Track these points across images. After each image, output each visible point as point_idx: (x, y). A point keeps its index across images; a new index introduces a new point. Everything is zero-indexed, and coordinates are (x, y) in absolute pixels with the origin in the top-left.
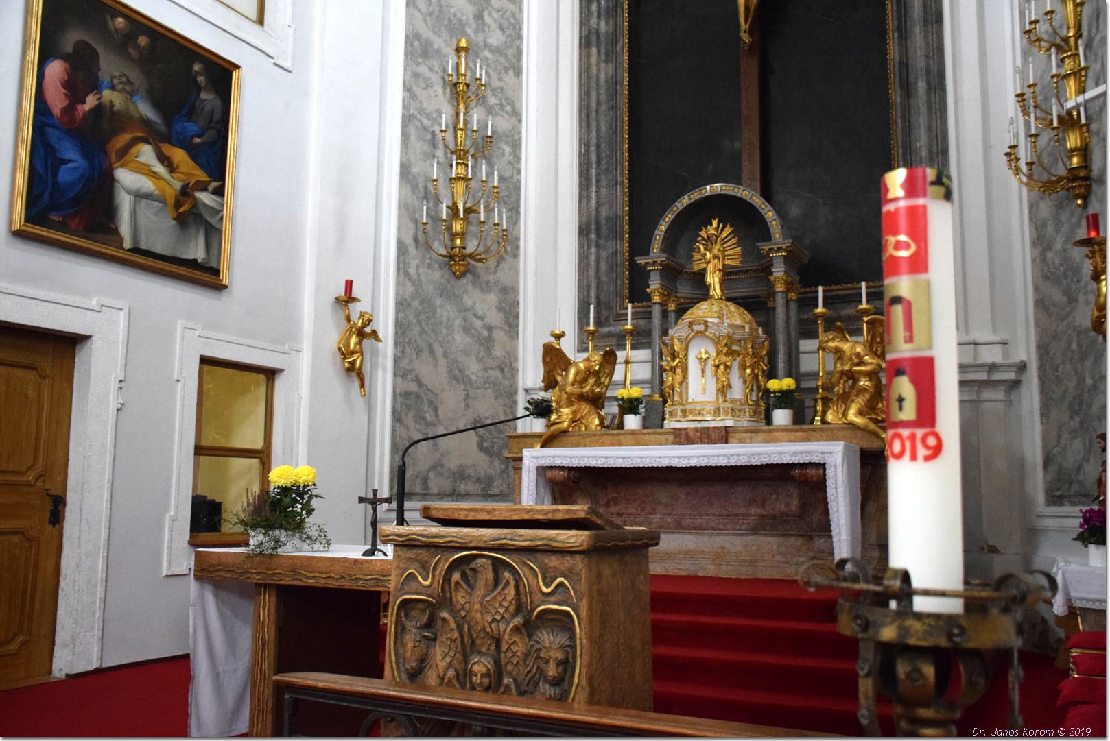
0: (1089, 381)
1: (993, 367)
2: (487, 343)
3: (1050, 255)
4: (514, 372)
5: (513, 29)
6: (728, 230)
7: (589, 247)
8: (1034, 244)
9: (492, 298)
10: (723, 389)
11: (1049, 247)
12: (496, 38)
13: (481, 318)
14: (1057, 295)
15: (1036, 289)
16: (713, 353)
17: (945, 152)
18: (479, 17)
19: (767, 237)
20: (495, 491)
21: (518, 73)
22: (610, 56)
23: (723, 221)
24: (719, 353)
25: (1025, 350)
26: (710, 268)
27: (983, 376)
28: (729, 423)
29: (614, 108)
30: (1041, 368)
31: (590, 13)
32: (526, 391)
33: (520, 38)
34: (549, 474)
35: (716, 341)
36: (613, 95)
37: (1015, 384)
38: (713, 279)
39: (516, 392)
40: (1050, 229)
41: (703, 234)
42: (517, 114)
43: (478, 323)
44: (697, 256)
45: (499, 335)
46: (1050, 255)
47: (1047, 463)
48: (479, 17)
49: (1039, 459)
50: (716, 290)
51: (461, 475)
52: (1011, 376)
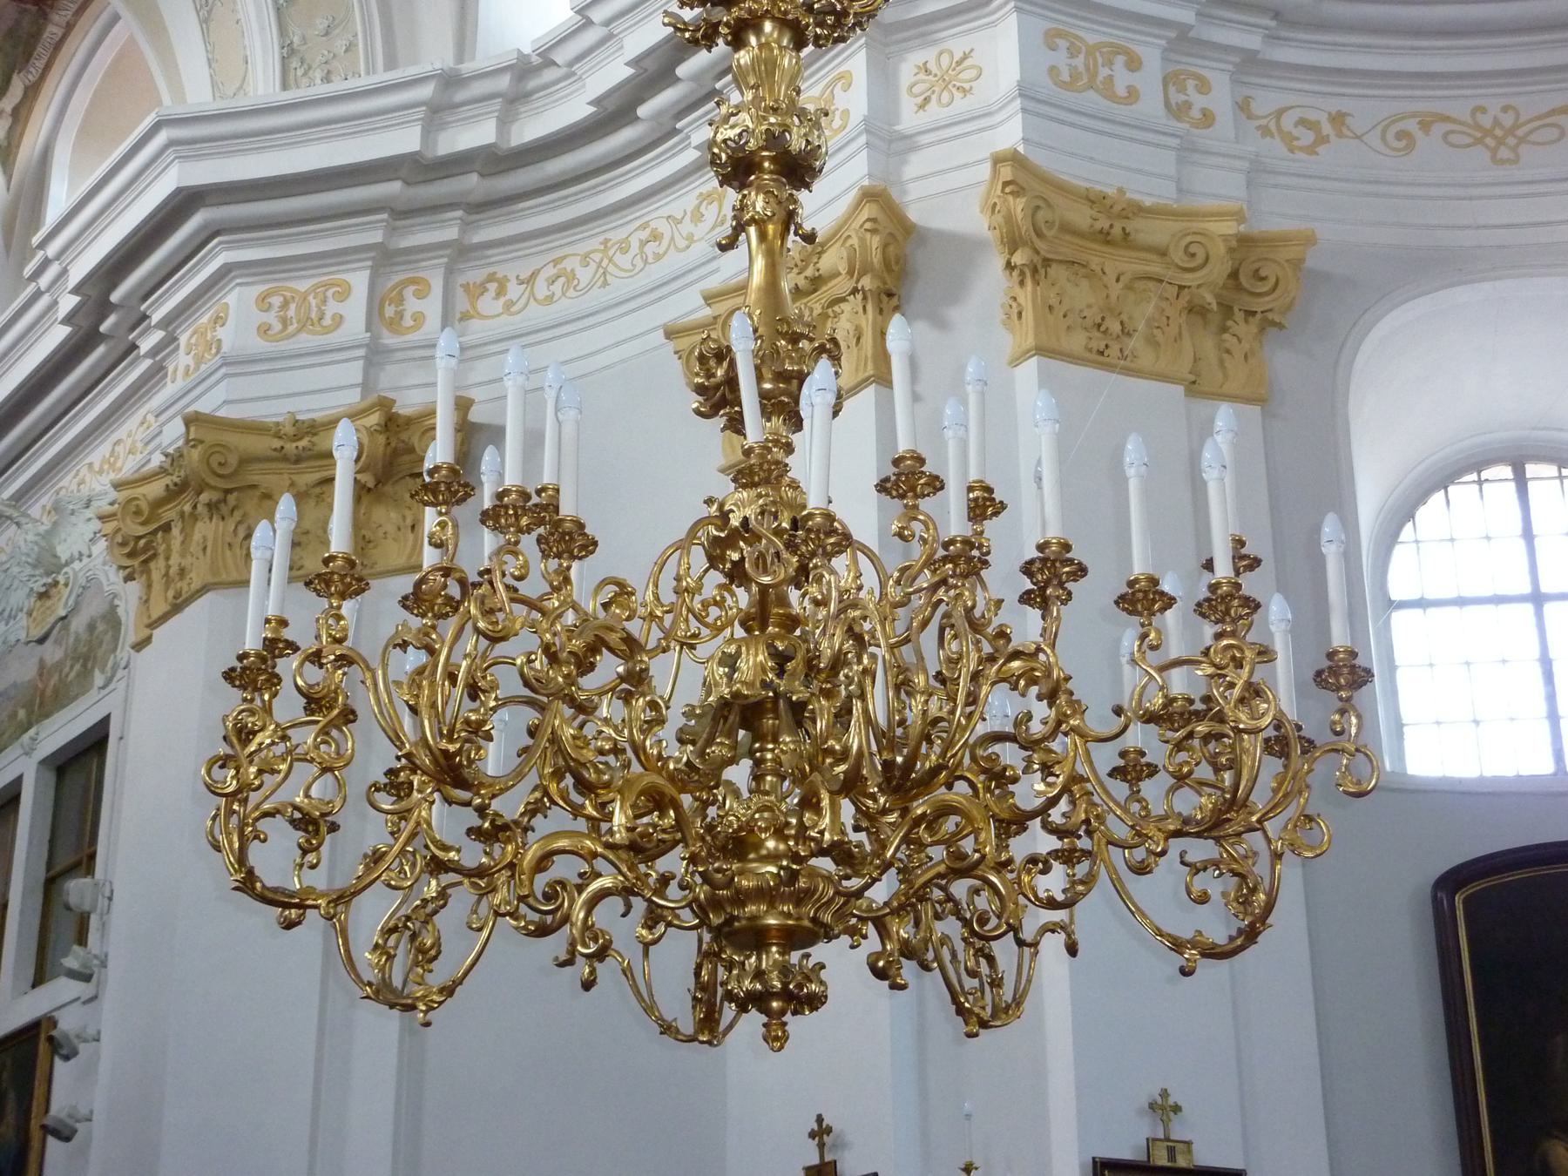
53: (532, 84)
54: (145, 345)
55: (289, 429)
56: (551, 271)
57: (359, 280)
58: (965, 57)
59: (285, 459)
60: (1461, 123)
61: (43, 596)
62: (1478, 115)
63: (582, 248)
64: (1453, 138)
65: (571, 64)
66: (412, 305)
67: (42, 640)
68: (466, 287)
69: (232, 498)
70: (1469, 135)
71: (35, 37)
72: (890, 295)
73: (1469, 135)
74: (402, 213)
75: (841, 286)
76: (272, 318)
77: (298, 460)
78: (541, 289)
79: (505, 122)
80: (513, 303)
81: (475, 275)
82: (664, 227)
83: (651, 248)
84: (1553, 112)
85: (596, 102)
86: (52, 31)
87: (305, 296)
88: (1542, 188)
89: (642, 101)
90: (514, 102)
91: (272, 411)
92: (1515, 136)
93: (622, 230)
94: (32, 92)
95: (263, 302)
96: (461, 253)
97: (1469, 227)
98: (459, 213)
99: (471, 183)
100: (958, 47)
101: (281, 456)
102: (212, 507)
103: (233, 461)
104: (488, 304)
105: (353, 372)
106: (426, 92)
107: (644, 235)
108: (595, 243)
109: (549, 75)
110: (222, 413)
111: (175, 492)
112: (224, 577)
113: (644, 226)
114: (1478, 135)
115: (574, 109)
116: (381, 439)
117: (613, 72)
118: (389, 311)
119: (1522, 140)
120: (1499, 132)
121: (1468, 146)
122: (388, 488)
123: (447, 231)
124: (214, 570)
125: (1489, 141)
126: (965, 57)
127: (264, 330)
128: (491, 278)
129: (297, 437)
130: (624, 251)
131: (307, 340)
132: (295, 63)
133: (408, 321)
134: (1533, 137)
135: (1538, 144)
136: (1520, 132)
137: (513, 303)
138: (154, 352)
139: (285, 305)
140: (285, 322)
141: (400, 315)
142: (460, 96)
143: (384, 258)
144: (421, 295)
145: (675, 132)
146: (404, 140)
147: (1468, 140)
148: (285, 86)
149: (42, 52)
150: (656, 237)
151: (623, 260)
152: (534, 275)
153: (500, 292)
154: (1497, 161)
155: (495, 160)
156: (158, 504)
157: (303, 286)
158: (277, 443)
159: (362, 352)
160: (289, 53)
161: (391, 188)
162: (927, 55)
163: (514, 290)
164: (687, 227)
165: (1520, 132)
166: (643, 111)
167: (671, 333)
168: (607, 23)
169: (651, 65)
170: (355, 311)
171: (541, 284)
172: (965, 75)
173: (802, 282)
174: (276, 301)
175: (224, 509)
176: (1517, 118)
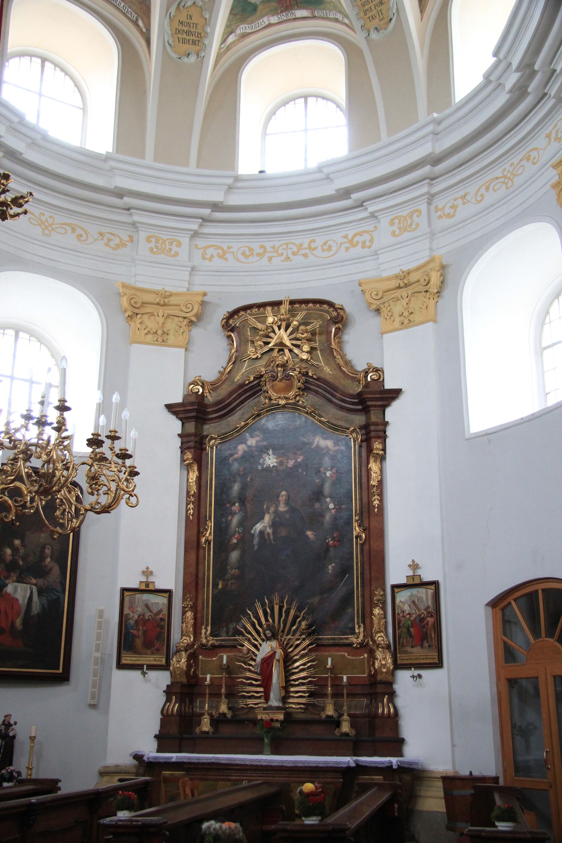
60: (35, 216)
62: (42, 216)
64: (31, 220)
70: (37, 222)
73: (37, 222)
84: (65, 224)
88: (56, 248)
92: (51, 227)
97: (30, 253)
114: (40, 222)
119: (53, 229)
120: (46, 224)
121: (34, 225)
125: (43, 226)
134: (57, 230)
135: (60, 233)
136: (54, 227)
147: (37, 223)
154: (44, 234)
165: (54, 227)
176: (54, 221)
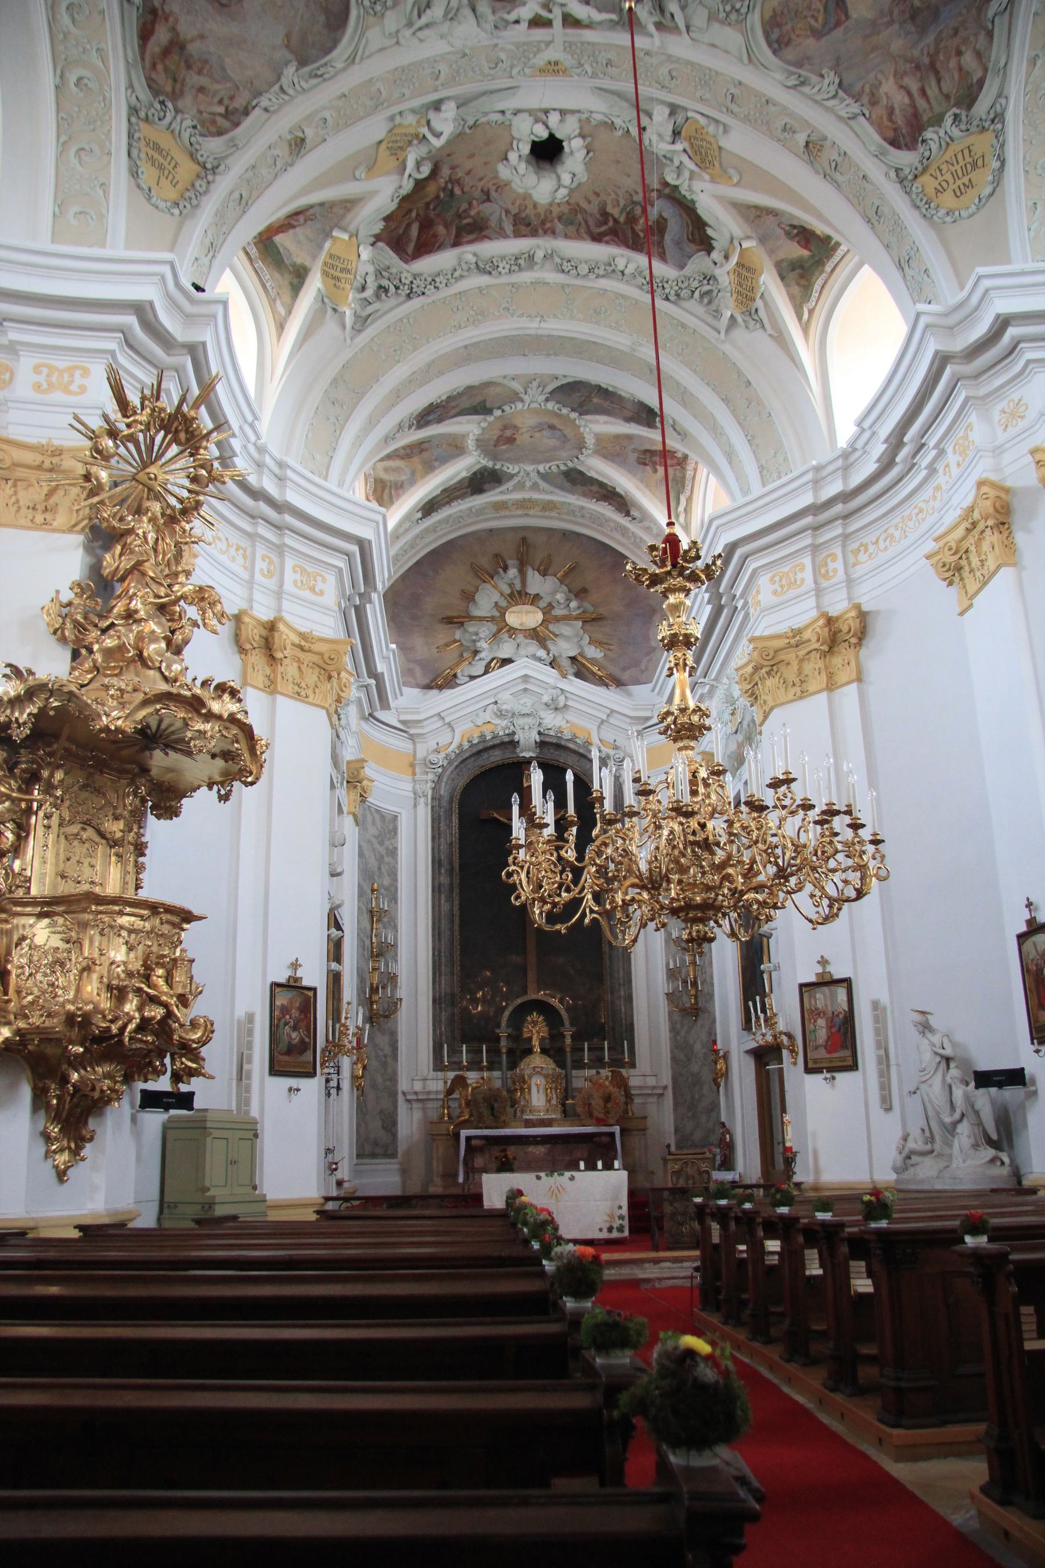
0: (697, 1096)
1: (654, 1088)
2: (384, 1065)
3: (678, 1038)
4: (396, 1081)
5: (393, 874)
6: (541, 1018)
7: (441, 1012)
8: (670, 1031)
9: (386, 1038)
10: (549, 1101)
11: (678, 1033)
12: (387, 881)
13: (382, 1050)
14: (682, 1057)
15: (672, 1052)
16: (543, 1081)
17: (630, 981)
18: (379, 868)
19: (563, 1025)
20: (389, 1152)
21: (396, 902)
22: (450, 899)
23: (539, 1013)
24: (547, 1082)
25: (666, 1079)
26: (535, 1038)
27: (650, 1092)
28: (553, 1116)
29: (452, 930)
30: (674, 1088)
31: (440, 872)
32: (404, 1094)
33: (396, 880)
34: (474, 1142)
35: (546, 1077)
36: (452, 922)
37: (662, 1095)
38: (536, 1042)
39: (396, 1094)
40: (678, 1026)
41: (529, 1018)
42: (395, 928)
43: (380, 1053)
44: (525, 1030)
45: (389, 1060)
46: (678, 1038)
47: (676, 1131)
48: (379, 868)
49: (672, 1130)
50: (537, 1049)
51: (376, 1143)
52: (660, 1091)
53: (852, 459)
54: (740, 605)
55: (791, 634)
56: (884, 536)
57: (807, 561)
58: (1020, 401)
59: (792, 646)
61: (733, 714)
63: (894, 522)
65: (863, 448)
66: (831, 566)
67: (736, 732)
68: (852, 551)
69: (775, 668)
71: (684, 478)
72: (1003, 524)
74: (816, 528)
75: (981, 526)
76: (777, 586)
77: (797, 646)
78: (882, 545)
79: (845, 478)
80: (871, 554)
81: (854, 546)
82: (922, 505)
83: (920, 516)
85: (878, 461)
86: (689, 474)
87: (787, 573)
89: (896, 455)
90: (846, 469)
91: (783, 628)
93: (907, 510)
94: (689, 500)
95: (772, 581)
96: (846, 537)
98: (840, 521)
99: (839, 508)
100: (1015, 397)
101: (789, 646)
102: (768, 673)
103: (772, 653)
104: (862, 557)
105: (812, 602)
106: (809, 476)
107: (916, 511)
108: (898, 519)
109: (857, 454)
110: (766, 633)
111: (756, 669)
112: (778, 702)
113: (915, 507)
115: (869, 467)
116: (826, 630)
117: (879, 449)
118: (823, 571)
122: (836, 649)
123: (837, 530)
124: (774, 700)
126: (1020, 401)
127: (775, 592)
128: (862, 545)
129: (794, 637)
130: (911, 520)
131: (792, 593)
132: (765, 472)
133: (831, 574)
137: (871, 554)
138: (743, 607)
139: (781, 580)
140: (782, 587)
141: (827, 571)
142: (825, 473)
143: (815, 549)
144: (834, 560)
145: (914, 465)
146: (806, 499)
148: (764, 486)
149: (688, 483)
150: (921, 511)
151: (911, 524)
152: (877, 540)
153: (866, 551)
155: (845, 497)
156: (753, 674)
157: (786, 569)
158: (787, 641)
159: (813, 593)
160: (762, 469)
161: (808, 520)
162: (1003, 404)
163: (871, 548)
164: (932, 503)
166: (898, 459)
167: (928, 557)
168: (871, 427)
169: (893, 440)
170: (808, 575)
171: (881, 542)
172: (1022, 409)
173: (969, 526)
174: (777, 578)
175: (773, 673)
